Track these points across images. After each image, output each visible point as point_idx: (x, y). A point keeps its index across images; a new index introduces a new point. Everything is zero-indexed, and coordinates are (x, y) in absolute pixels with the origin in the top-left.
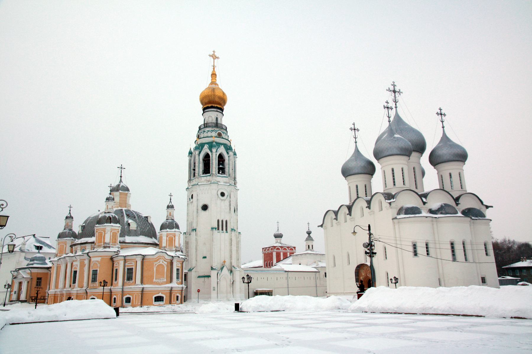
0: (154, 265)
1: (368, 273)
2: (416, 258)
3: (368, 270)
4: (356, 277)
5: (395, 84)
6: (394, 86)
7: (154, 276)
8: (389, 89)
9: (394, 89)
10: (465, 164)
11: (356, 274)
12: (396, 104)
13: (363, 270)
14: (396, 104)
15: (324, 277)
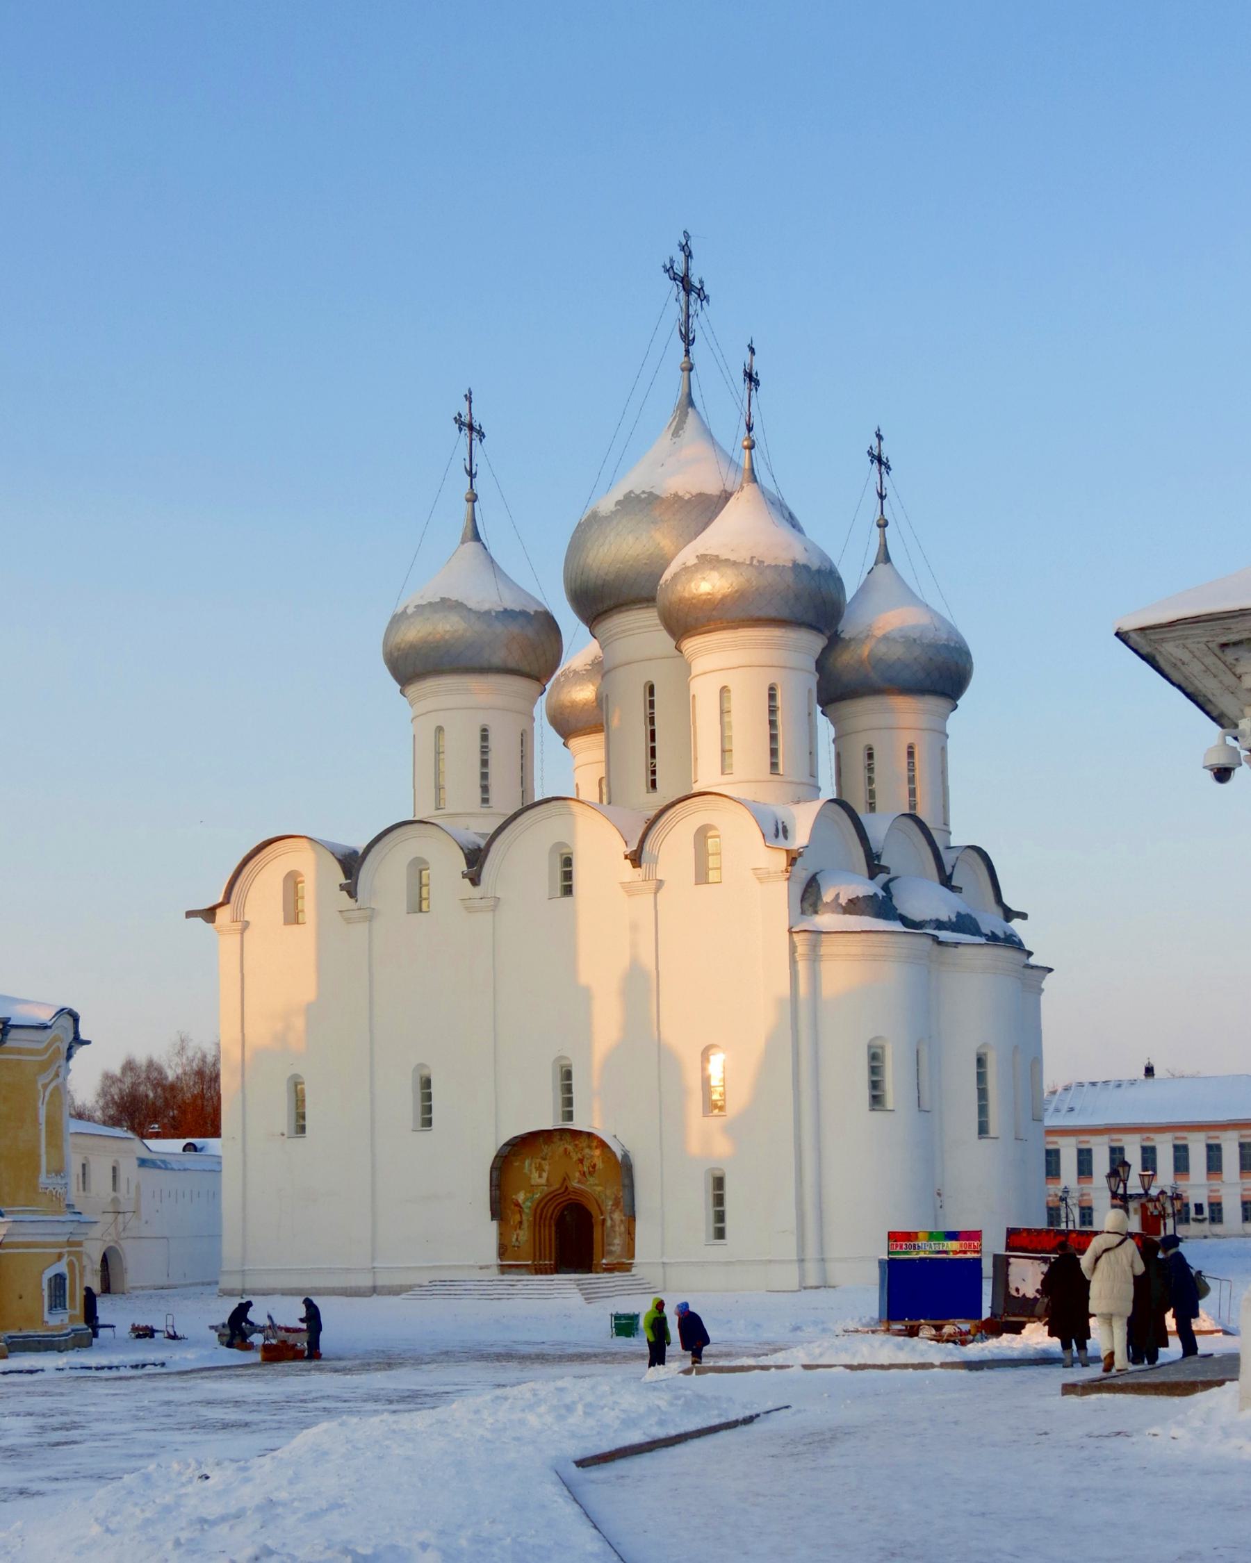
0: (40, 1087)
1: (577, 1174)
2: (877, 1115)
3: (581, 1161)
4: (493, 1192)
5: (693, 245)
6: (689, 256)
7: (39, 1156)
8: (672, 267)
9: (687, 269)
10: (955, 707)
11: (494, 1175)
12: (687, 352)
13: (538, 1160)
14: (687, 352)
15: (78, 1190)
